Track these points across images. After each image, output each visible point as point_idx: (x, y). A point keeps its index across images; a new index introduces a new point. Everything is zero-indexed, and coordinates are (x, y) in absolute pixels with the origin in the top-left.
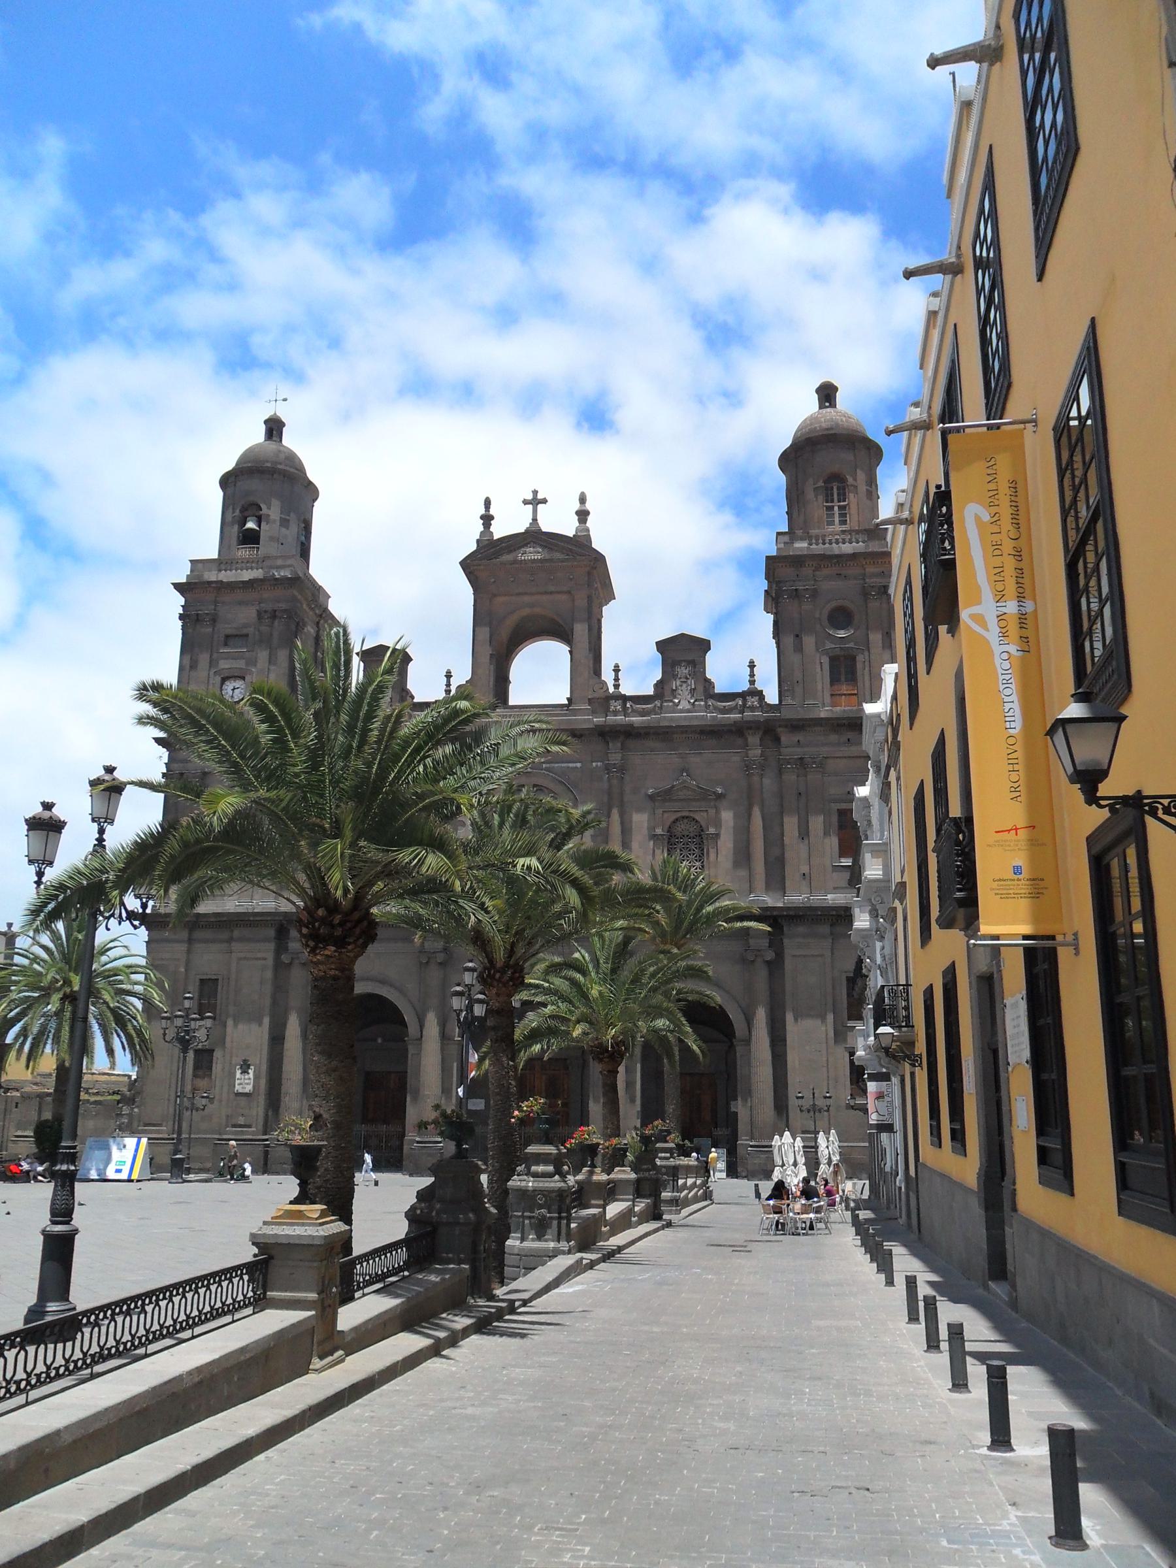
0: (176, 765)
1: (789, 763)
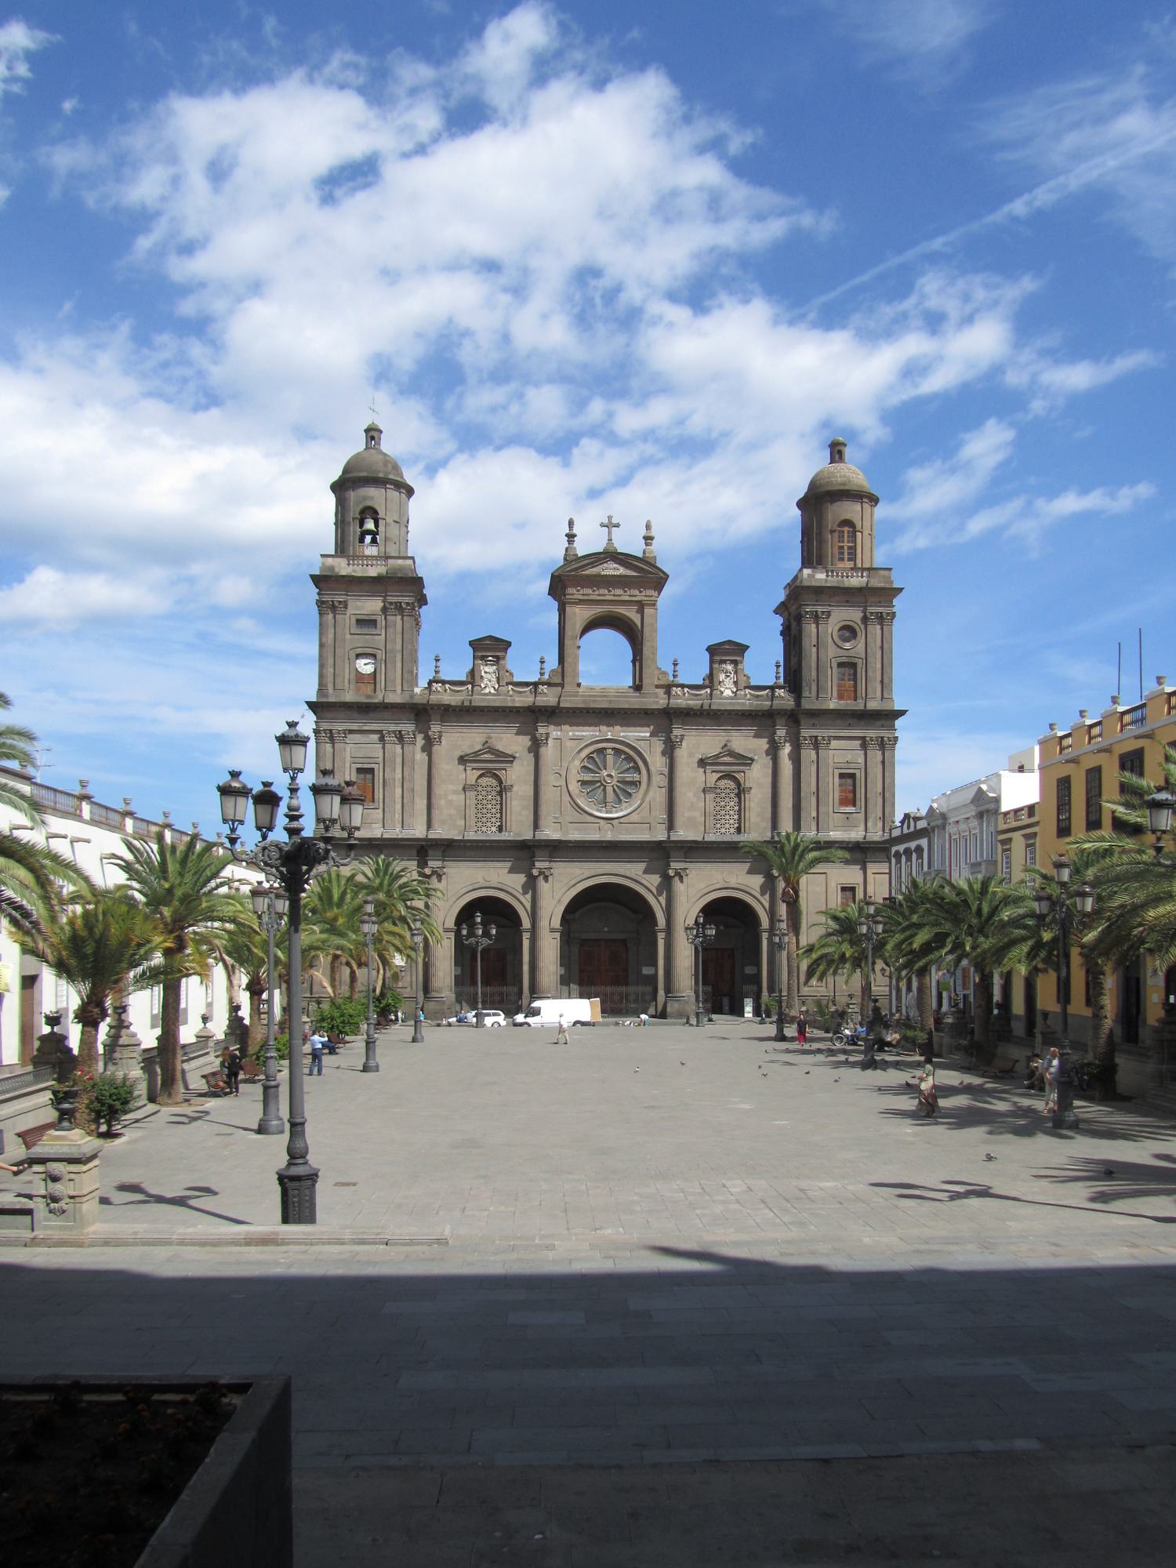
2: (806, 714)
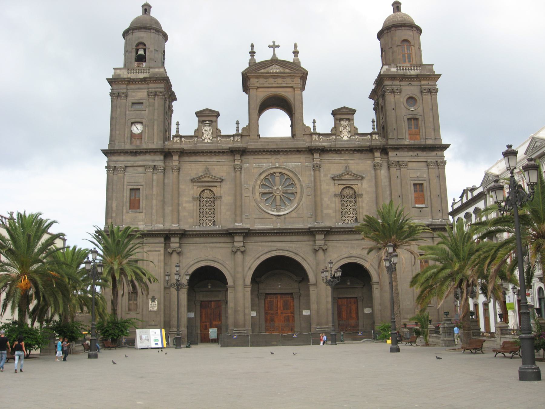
0: (112, 163)
1: (393, 164)
2: (391, 148)
